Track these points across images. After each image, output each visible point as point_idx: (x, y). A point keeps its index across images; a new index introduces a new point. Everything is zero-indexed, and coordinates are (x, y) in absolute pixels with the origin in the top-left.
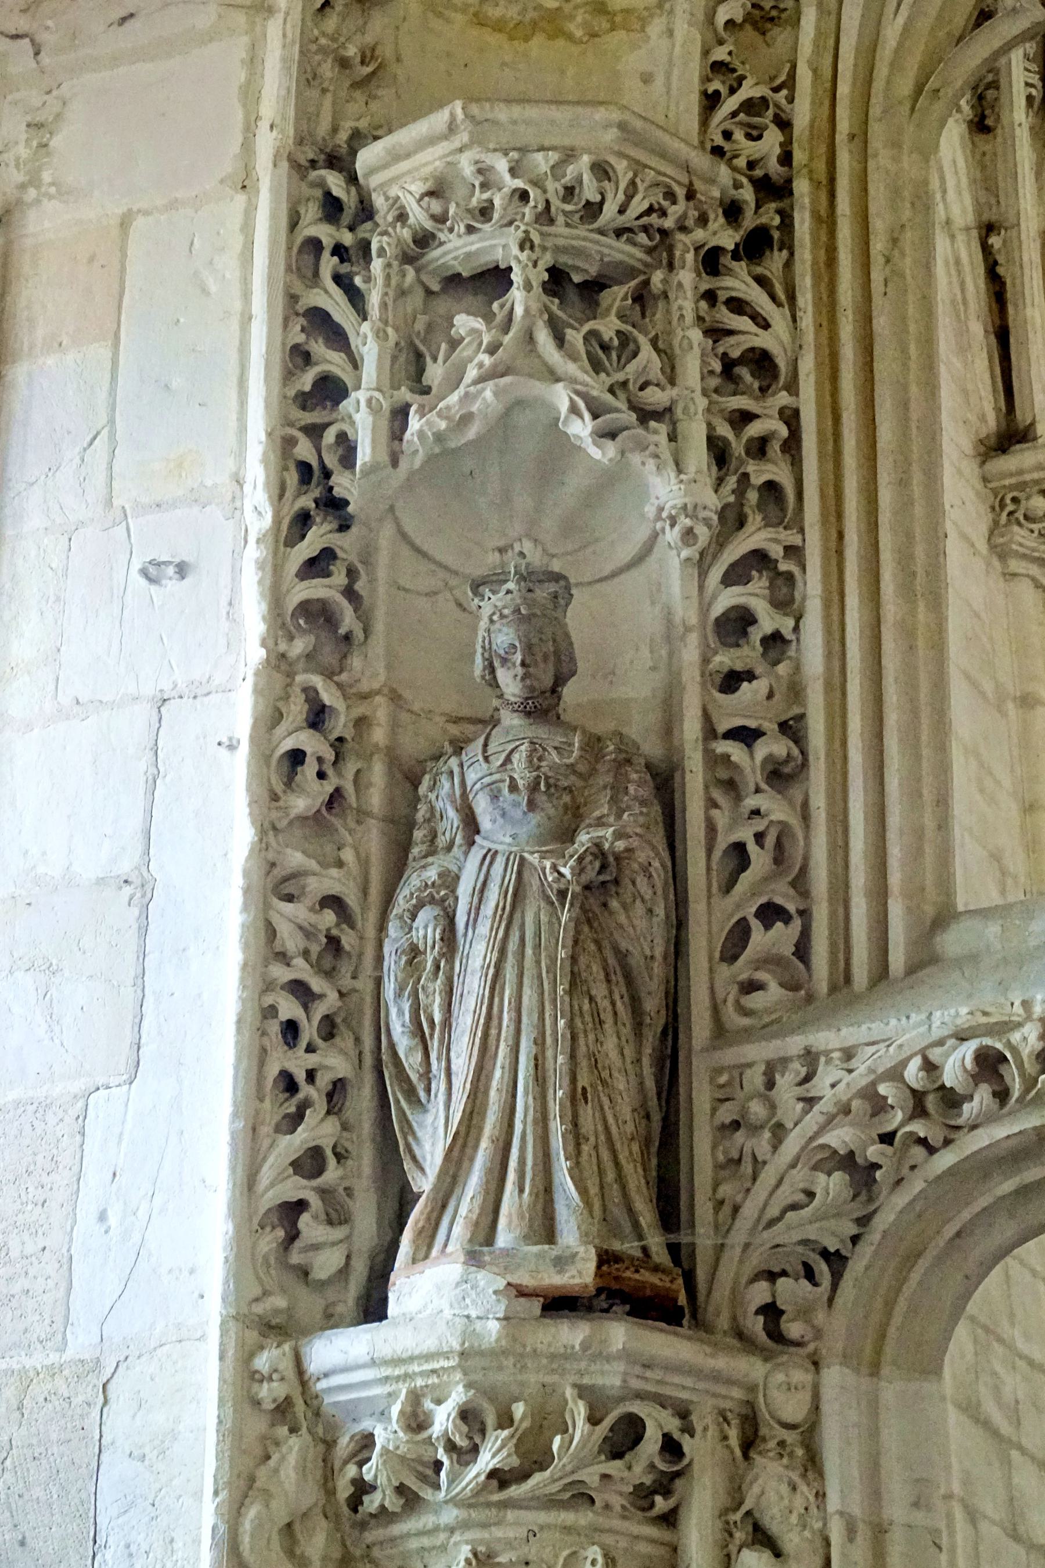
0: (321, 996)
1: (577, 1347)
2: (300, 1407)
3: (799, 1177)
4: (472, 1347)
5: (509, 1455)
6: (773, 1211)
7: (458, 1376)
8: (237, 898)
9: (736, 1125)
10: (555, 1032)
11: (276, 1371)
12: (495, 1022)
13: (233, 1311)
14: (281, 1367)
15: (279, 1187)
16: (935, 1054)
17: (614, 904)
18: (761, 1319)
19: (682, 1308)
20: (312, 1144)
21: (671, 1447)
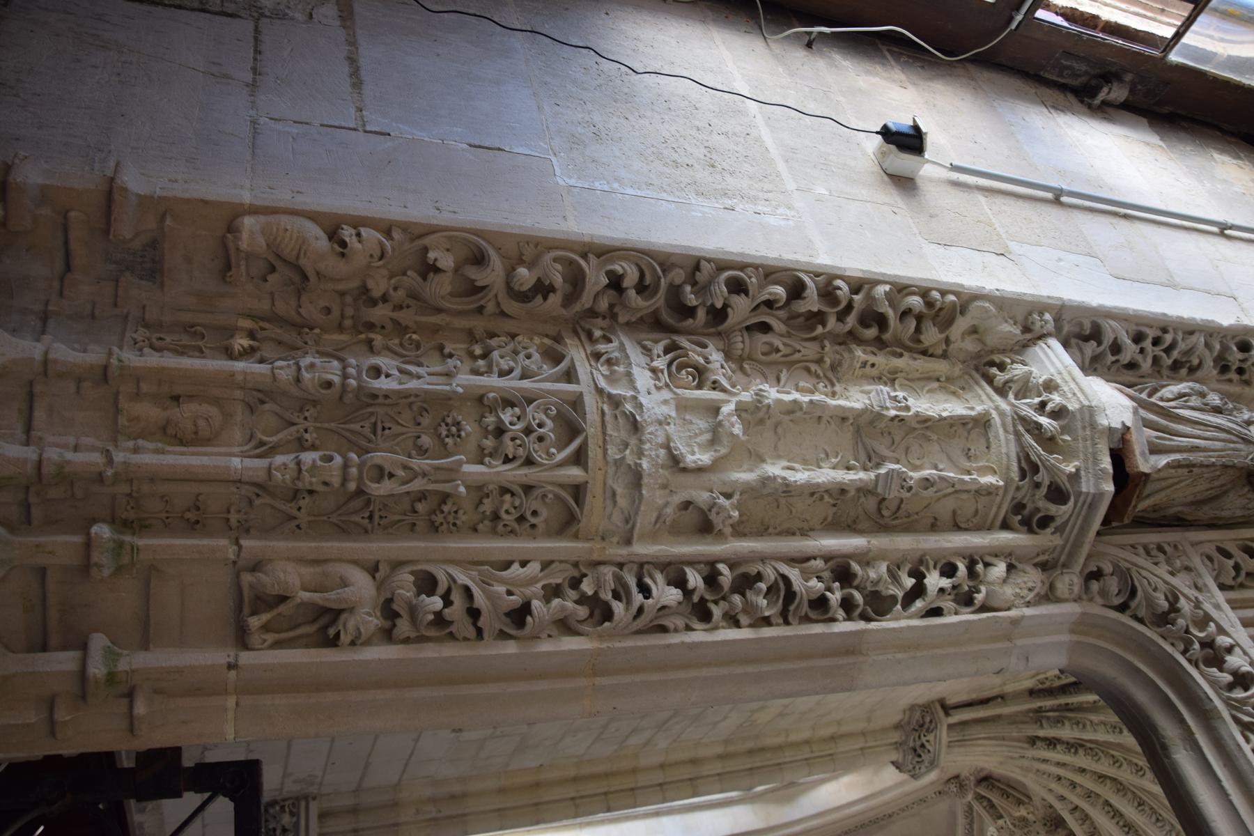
0: (1169, 357)
1: (1102, 466)
2: (1028, 336)
3: (1160, 584)
4: (1095, 411)
5: (1051, 431)
6: (1144, 573)
7: (1077, 406)
8: (1205, 317)
9: (1165, 553)
10: (1211, 457)
11: (1046, 323)
12: (1205, 428)
13: (1066, 303)
14: (1048, 325)
15: (1109, 330)
16: (1237, 649)
17: (1246, 489)
18: (1095, 569)
19: (1111, 524)
20: (1124, 346)
21: (1045, 522)
